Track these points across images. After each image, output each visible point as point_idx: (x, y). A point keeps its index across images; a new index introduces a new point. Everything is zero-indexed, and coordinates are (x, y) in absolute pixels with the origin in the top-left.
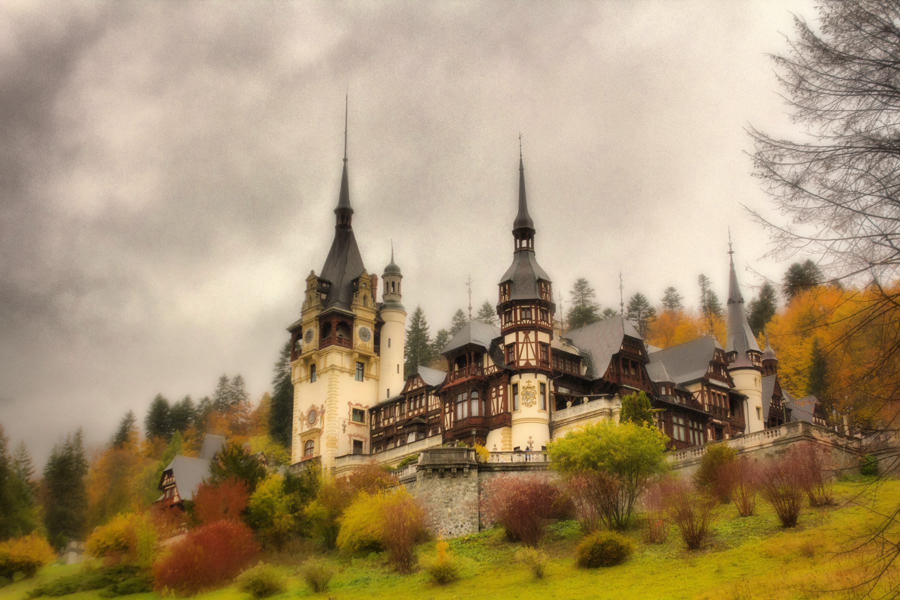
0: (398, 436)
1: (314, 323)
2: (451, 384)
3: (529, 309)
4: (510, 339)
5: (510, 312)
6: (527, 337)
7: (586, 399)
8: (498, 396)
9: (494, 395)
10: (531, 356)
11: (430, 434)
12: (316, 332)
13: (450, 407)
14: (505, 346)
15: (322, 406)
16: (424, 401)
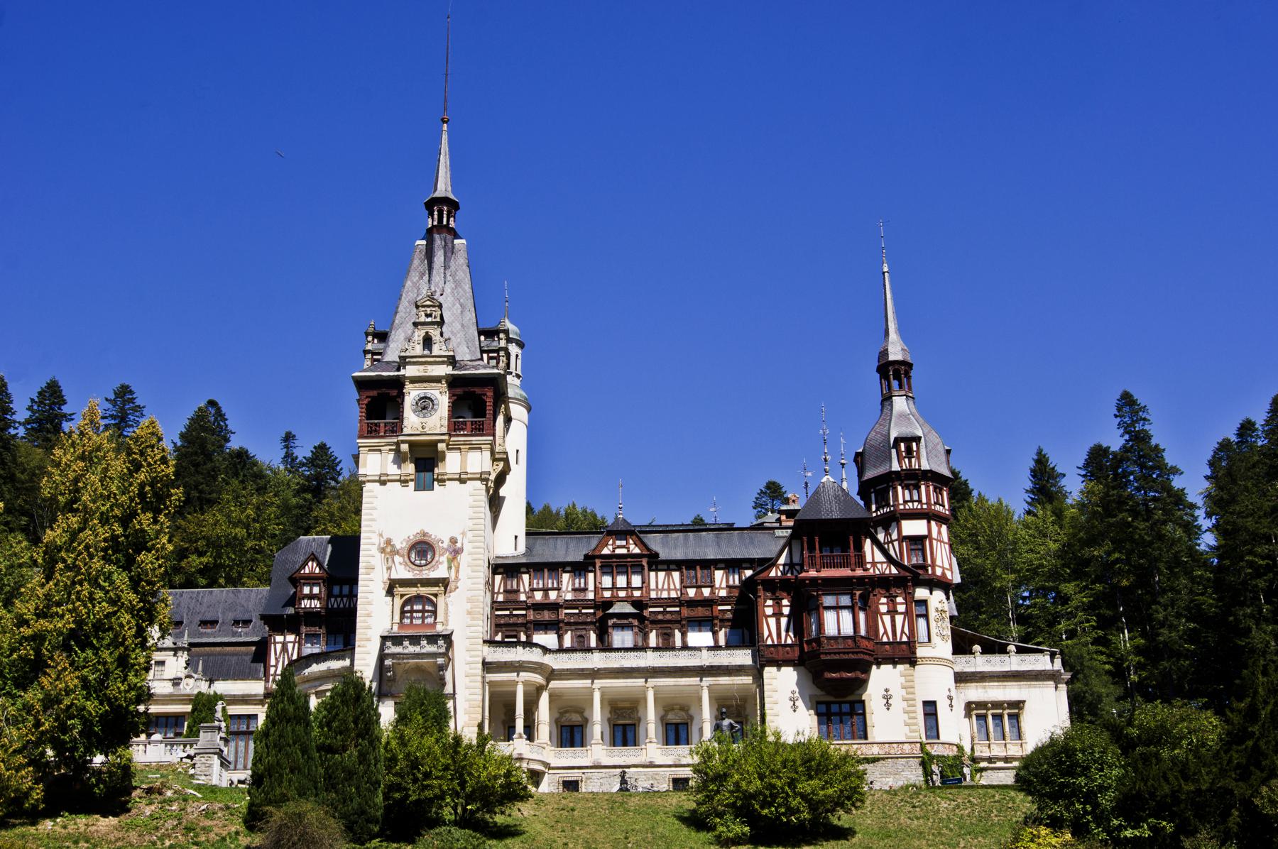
0: (569, 624)
1: (444, 385)
2: (813, 573)
3: (941, 490)
4: (913, 528)
5: (918, 488)
6: (939, 533)
7: (1012, 648)
8: (893, 612)
9: (883, 609)
10: (947, 566)
11: (653, 639)
12: (443, 400)
13: (778, 604)
14: (902, 539)
15: (453, 541)
16: (636, 580)
